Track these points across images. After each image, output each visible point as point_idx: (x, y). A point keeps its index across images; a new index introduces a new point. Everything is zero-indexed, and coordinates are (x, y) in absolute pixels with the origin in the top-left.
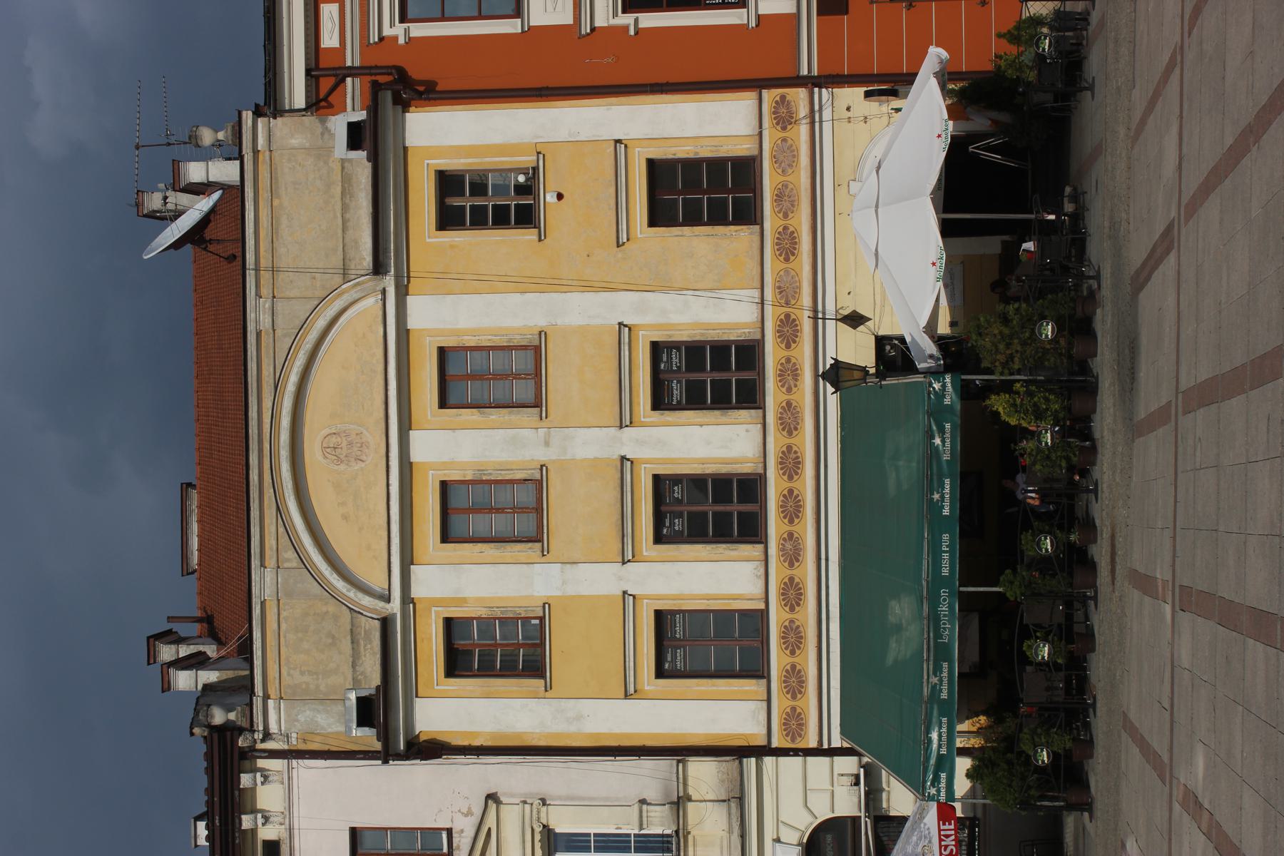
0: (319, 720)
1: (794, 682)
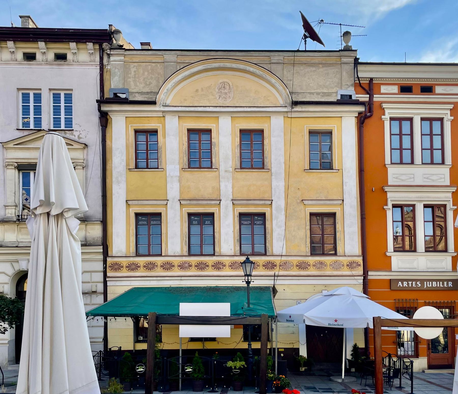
0: (116, 78)
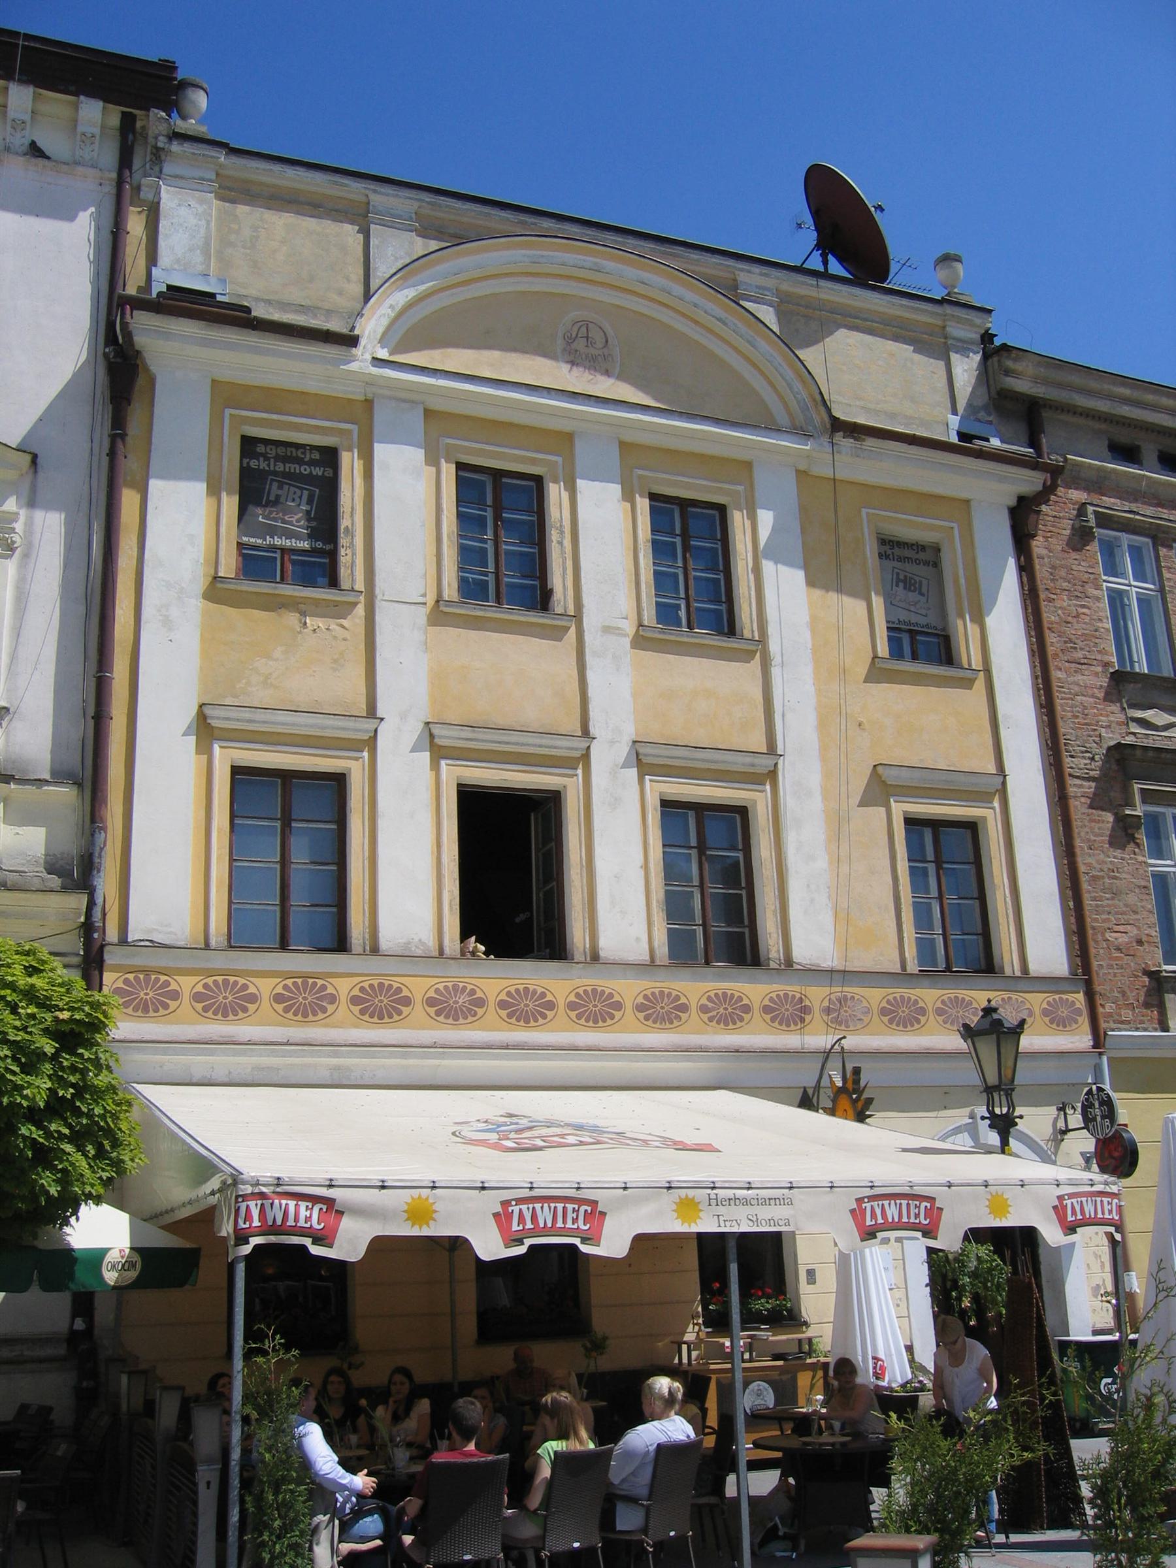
1: (225, 998)
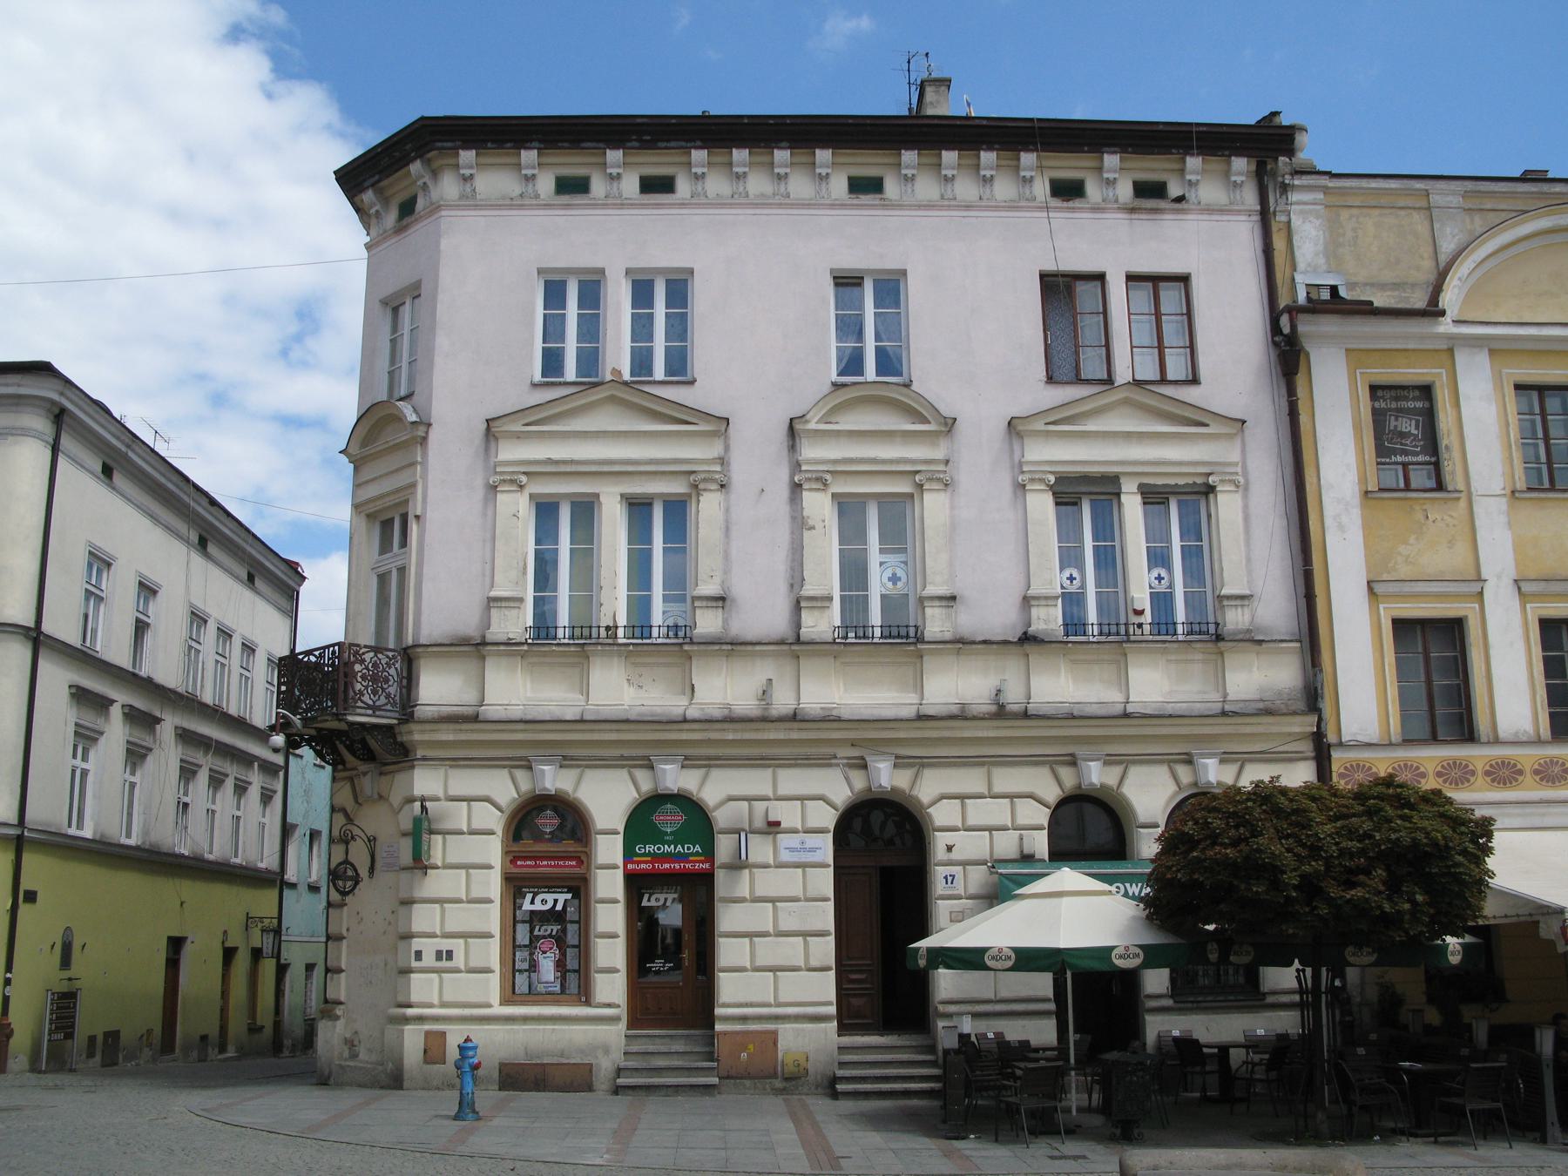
1: (1406, 776)
